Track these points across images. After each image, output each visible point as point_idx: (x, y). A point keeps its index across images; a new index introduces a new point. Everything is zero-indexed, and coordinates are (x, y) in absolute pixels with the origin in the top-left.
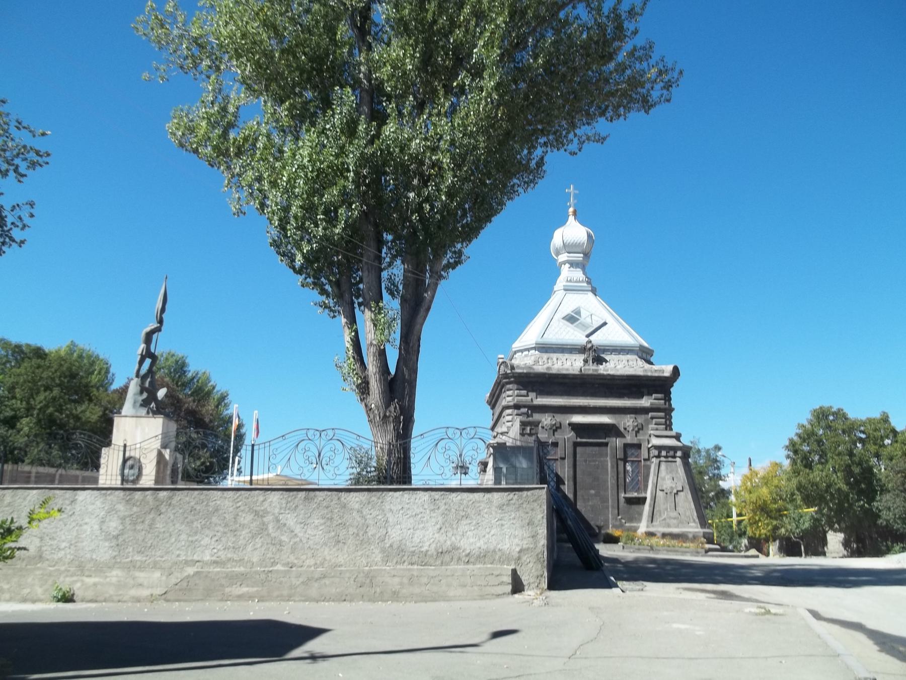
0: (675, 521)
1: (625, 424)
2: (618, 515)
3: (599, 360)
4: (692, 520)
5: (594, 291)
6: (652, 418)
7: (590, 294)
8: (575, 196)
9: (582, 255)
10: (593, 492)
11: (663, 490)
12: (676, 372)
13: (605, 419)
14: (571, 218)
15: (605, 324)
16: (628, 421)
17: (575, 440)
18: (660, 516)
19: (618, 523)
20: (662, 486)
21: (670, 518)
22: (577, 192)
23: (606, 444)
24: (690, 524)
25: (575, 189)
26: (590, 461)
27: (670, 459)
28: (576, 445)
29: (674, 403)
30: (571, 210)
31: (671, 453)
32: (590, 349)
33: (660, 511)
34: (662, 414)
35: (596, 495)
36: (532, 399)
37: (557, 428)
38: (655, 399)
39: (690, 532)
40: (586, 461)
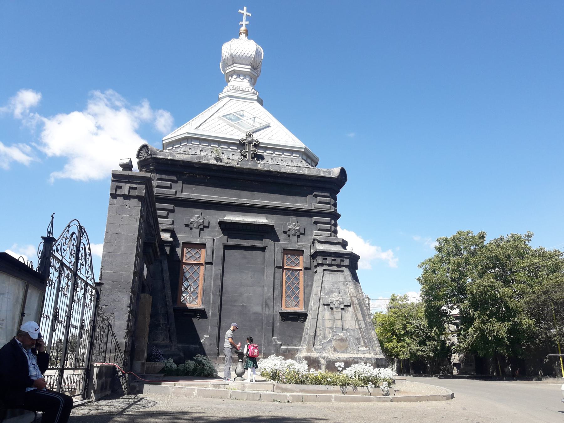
1: (285, 227)
2: (273, 336)
5: (260, 101)
6: (316, 223)
7: (256, 103)
8: (248, 18)
9: (250, 67)
11: (328, 305)
12: (343, 171)
14: (243, 36)
15: (269, 126)
17: (226, 242)
23: (263, 249)
25: (247, 11)
27: (335, 268)
28: (227, 247)
30: (243, 29)
31: (338, 261)
32: (250, 143)
34: (327, 219)
36: (176, 192)
37: (205, 227)
38: (320, 203)
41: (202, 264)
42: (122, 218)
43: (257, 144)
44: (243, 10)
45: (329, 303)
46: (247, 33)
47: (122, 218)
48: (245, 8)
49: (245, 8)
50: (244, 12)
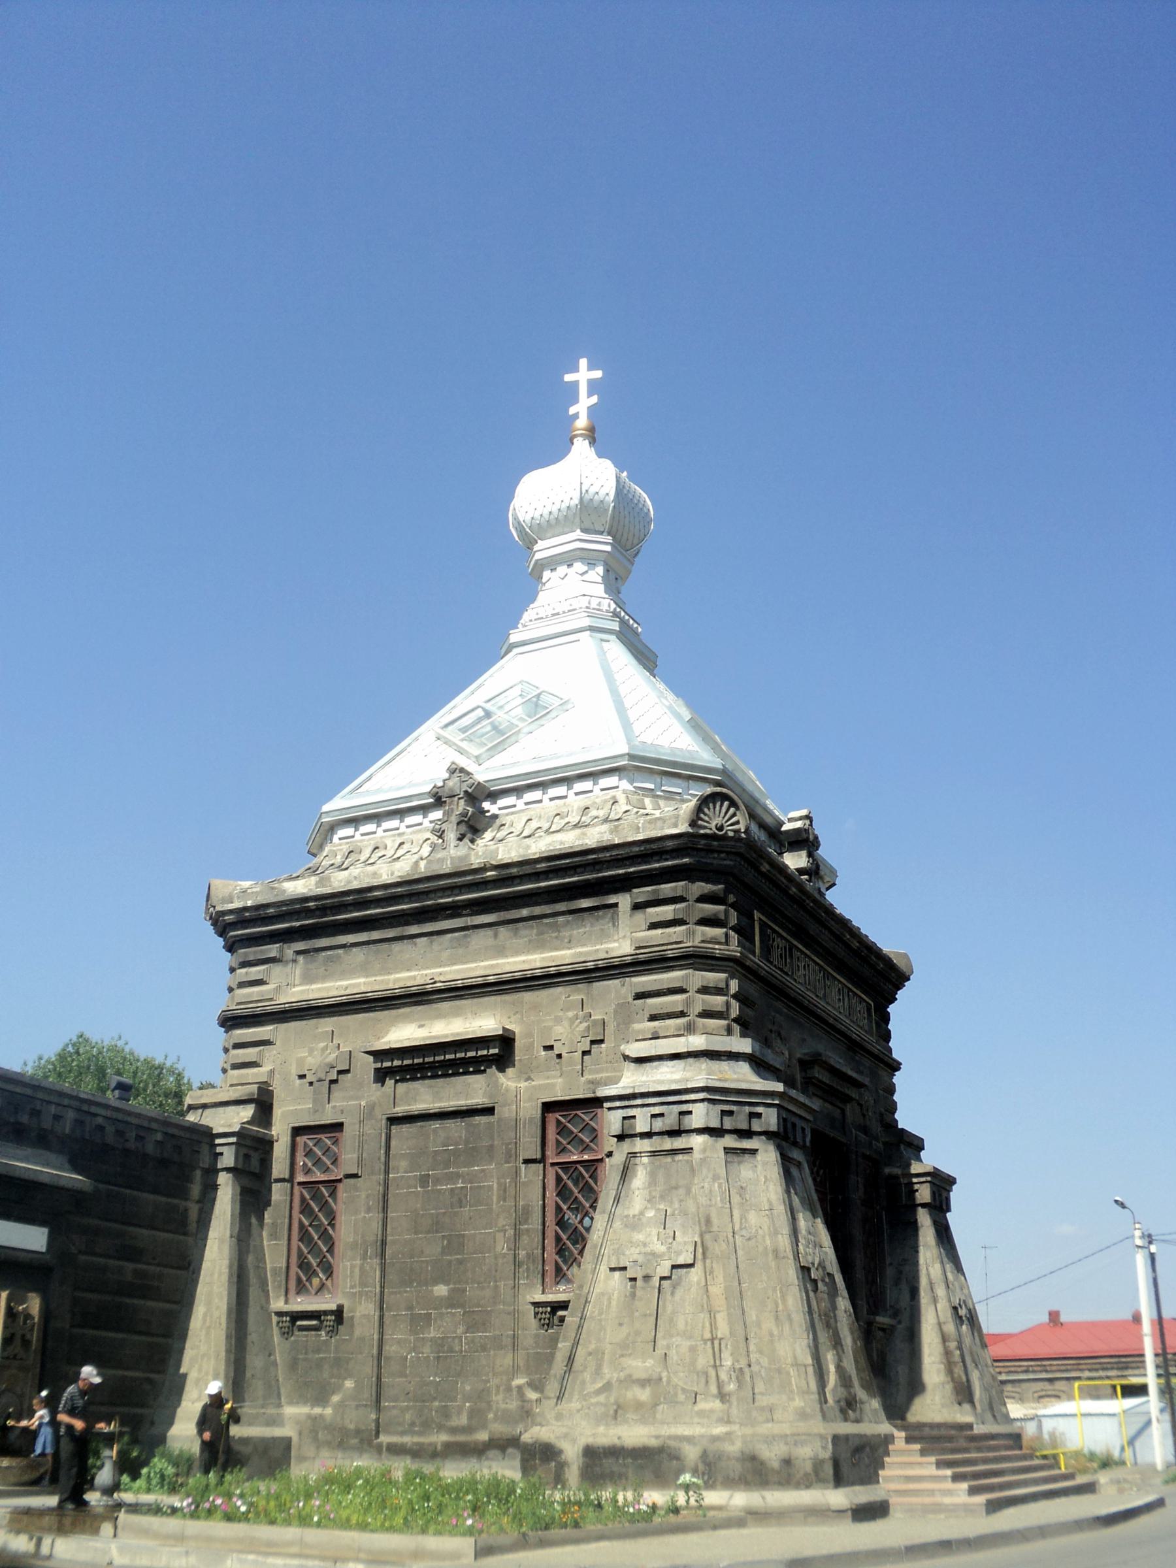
0: (644, 1395)
3: (473, 826)
4: (713, 1389)
10: (441, 1290)
14: (581, 446)
16: (558, 1020)
18: (598, 1371)
19: (513, 1405)
20: (618, 1252)
21: (630, 1381)
24: (702, 1405)
25: (590, 368)
26: (437, 1181)
33: (598, 1354)
35: (452, 1301)
38: (654, 926)
39: (689, 1439)
40: (424, 1180)
41: (340, 1181)
44: (590, 368)
45: (627, 1264)
46: (592, 435)
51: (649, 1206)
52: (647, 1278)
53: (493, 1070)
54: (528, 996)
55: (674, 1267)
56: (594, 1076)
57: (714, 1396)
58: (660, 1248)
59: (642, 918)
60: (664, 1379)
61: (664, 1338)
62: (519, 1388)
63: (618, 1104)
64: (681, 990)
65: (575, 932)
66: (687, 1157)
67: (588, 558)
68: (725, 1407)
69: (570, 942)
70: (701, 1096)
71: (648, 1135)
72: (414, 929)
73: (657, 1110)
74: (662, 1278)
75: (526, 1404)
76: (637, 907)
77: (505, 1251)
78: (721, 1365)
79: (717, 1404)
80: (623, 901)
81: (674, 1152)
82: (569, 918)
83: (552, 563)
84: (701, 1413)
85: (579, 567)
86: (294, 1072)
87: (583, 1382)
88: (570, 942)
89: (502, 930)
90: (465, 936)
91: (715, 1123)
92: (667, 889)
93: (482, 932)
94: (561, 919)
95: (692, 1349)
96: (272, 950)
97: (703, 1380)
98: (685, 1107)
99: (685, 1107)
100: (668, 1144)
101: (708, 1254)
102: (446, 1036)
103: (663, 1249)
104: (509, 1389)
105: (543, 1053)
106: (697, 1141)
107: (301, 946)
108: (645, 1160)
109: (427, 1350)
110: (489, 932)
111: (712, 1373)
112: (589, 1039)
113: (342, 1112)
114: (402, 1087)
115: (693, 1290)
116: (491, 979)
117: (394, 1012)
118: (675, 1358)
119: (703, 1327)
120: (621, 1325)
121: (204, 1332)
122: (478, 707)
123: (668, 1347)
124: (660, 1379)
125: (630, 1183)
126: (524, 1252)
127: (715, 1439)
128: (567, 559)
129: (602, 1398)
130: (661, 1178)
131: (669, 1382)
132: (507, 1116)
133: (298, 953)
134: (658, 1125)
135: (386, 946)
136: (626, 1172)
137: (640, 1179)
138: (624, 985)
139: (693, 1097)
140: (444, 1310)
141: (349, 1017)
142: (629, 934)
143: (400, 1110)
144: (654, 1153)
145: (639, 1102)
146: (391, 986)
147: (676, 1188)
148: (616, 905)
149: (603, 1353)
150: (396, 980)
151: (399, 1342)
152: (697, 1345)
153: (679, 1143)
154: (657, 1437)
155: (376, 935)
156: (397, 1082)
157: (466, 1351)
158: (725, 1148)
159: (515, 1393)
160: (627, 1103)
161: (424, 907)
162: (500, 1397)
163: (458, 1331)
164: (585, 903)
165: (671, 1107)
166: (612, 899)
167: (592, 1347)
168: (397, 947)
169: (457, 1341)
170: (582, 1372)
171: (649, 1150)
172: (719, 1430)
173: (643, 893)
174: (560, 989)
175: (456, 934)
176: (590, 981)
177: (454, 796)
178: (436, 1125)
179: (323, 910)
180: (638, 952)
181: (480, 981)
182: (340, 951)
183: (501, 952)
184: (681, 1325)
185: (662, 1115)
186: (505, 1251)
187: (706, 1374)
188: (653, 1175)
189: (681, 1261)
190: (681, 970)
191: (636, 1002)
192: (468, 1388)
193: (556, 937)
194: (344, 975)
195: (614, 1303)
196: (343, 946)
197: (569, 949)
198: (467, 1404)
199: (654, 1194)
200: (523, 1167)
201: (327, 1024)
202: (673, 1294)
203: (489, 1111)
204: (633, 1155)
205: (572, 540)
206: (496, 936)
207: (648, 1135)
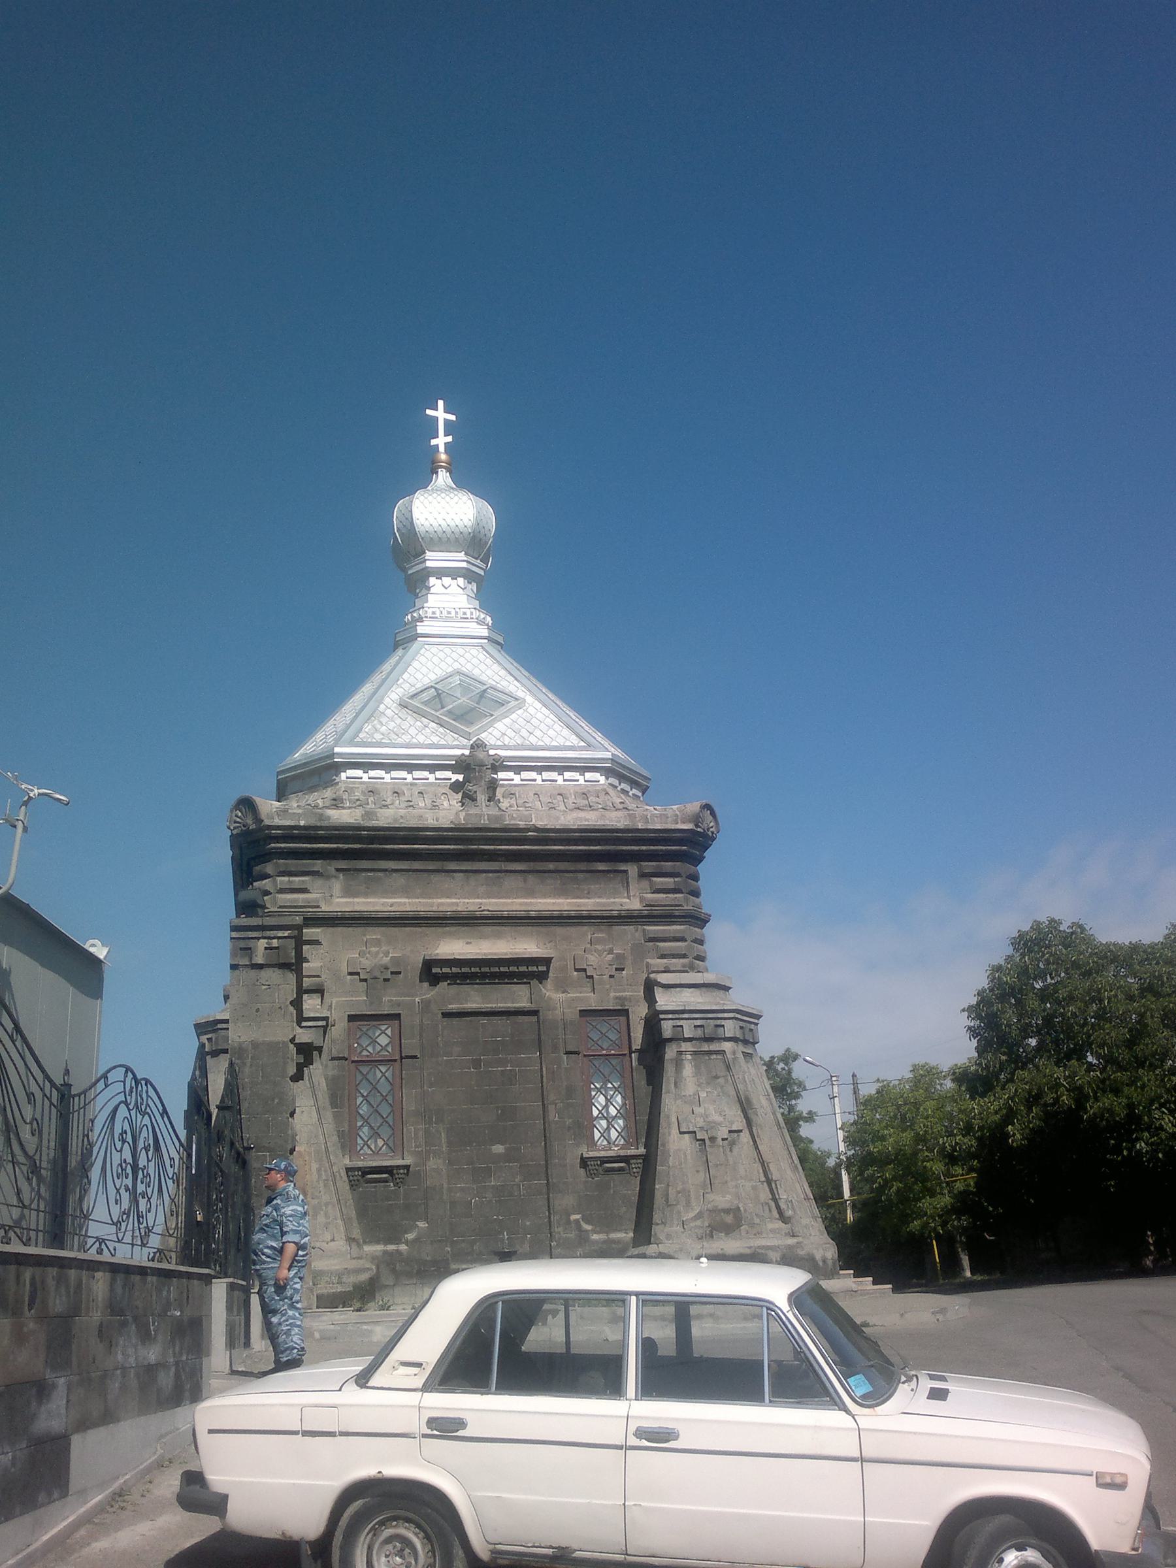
8: (450, 428)
10: (499, 1149)
13: (526, 946)
14: (443, 478)
18: (688, 1204)
22: (453, 418)
29: (706, 903)
35: (508, 1157)
40: (477, 1063)
42: (258, 1010)
43: (497, 764)
47: (258, 1010)
48: (441, 403)
49: (441, 403)
50: (440, 414)
51: (699, 1089)
52: (713, 1139)
53: (534, 982)
54: (560, 931)
55: (730, 1132)
56: (621, 994)
57: (777, 1219)
58: (716, 1118)
59: (645, 883)
60: (742, 1209)
61: (732, 1180)
62: (577, 1221)
63: (670, 1016)
64: (683, 939)
65: (592, 887)
66: (719, 1057)
67: (469, 575)
68: (788, 1226)
69: (589, 893)
70: (731, 1015)
71: (690, 1040)
72: (452, 866)
73: (698, 1023)
74: (723, 1140)
75: (583, 1233)
76: (643, 875)
77: (556, 1119)
78: (780, 1199)
79: (780, 1224)
80: (632, 869)
81: (710, 1053)
82: (588, 875)
83: (440, 573)
84: (772, 1231)
85: (461, 581)
86: (344, 969)
87: (679, 1212)
88: (589, 893)
89: (530, 877)
90: (498, 877)
91: (739, 1034)
92: (668, 865)
93: (513, 876)
94: (581, 875)
95: (754, 1188)
96: (318, 865)
97: (766, 1208)
98: (719, 1022)
99: (719, 1022)
100: (705, 1047)
101: (753, 1124)
102: (506, 954)
103: (721, 1119)
104: (568, 1222)
105: (576, 973)
106: (727, 1046)
107: (343, 864)
108: (689, 1057)
109: (489, 1195)
110: (519, 877)
111: (772, 1204)
112: (614, 966)
113: (399, 1005)
114: (454, 989)
115: (745, 1147)
116: (533, 914)
117: (440, 930)
118: (743, 1194)
119: (758, 1173)
120: (698, 1171)
121: (322, 1184)
122: (432, 687)
123: (736, 1187)
124: (739, 1208)
125: (682, 1072)
126: (570, 1120)
127: (790, 1247)
128: (453, 573)
129: (698, 1223)
130: (703, 1069)
131: (745, 1210)
132: (551, 1017)
133: (338, 870)
134: (699, 1033)
135: (426, 875)
136: (678, 1064)
137: (688, 1070)
138: (637, 930)
139: (726, 1015)
140: (502, 1164)
141: (396, 929)
142: (638, 894)
143: (453, 1007)
144: (695, 1053)
145: (686, 1016)
146: (435, 909)
147: (717, 1077)
148: (625, 872)
149: (689, 1192)
150: (439, 905)
151: (462, 1189)
152: (756, 1186)
153: (714, 1046)
154: (750, 1248)
155: (417, 865)
156: (448, 984)
157: (524, 1195)
158: (743, 1052)
159: (573, 1225)
160: (677, 1016)
161: (468, 850)
162: (561, 1229)
163: (516, 1180)
164: (601, 866)
165: (708, 1021)
166: (623, 867)
167: (680, 1187)
168: (435, 878)
169: (515, 1187)
170: (675, 1205)
171: (693, 1050)
172: (791, 1241)
173: (649, 866)
174: (586, 928)
175: (491, 875)
176: (611, 924)
177: (483, 766)
178: (484, 1020)
179: (372, 840)
180: (649, 908)
181: (523, 914)
182: (380, 874)
183: (531, 893)
184: (742, 1172)
185: (702, 1026)
186: (556, 1119)
187: (767, 1204)
188: (697, 1067)
189: (734, 1128)
190: (681, 925)
191: (647, 943)
192: (528, 1223)
193: (578, 889)
194: (386, 893)
195: (689, 1157)
196: (385, 870)
197: (589, 898)
198: (529, 1236)
199: (701, 1081)
200: (565, 1057)
201: (374, 934)
202: (731, 1150)
203: (535, 1013)
204: (680, 1053)
205: (457, 559)
206: (525, 881)
207: (690, 1040)
